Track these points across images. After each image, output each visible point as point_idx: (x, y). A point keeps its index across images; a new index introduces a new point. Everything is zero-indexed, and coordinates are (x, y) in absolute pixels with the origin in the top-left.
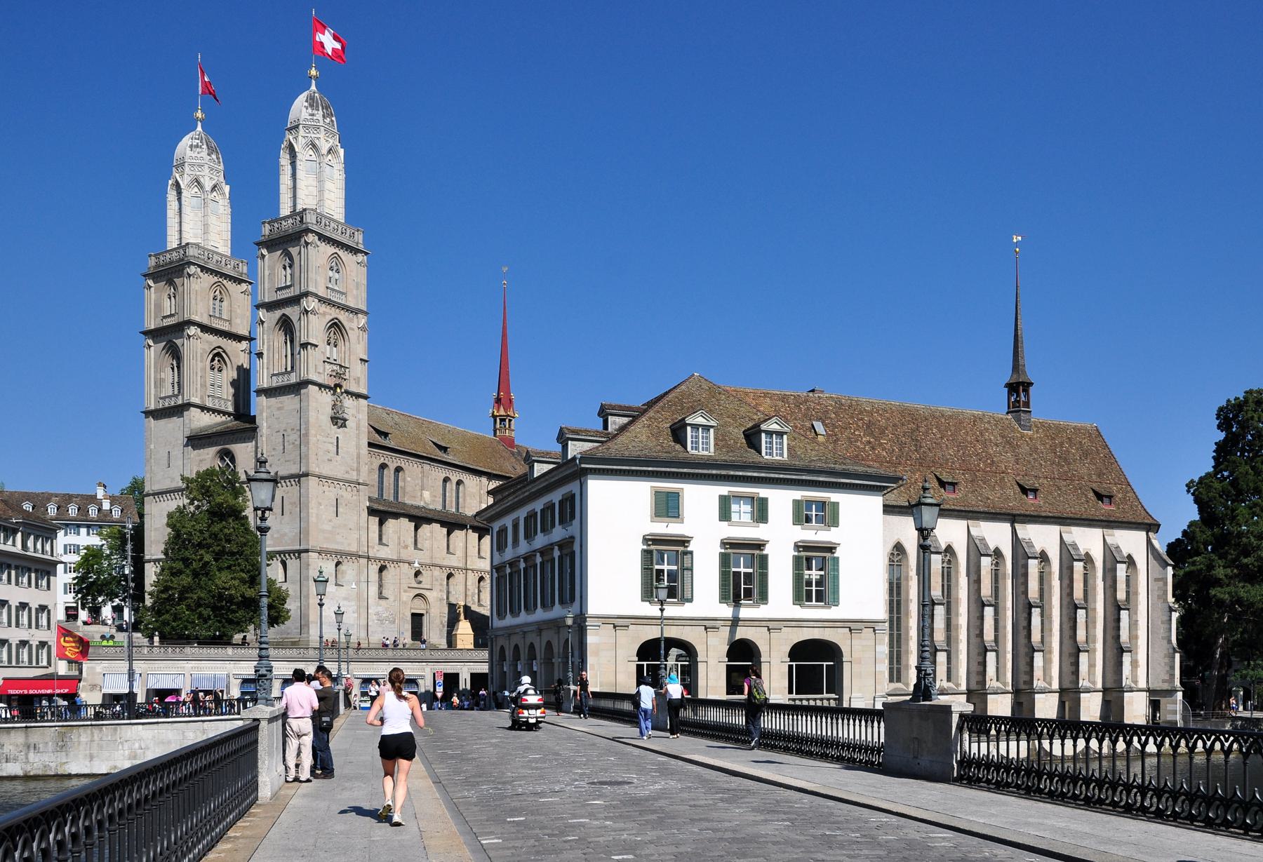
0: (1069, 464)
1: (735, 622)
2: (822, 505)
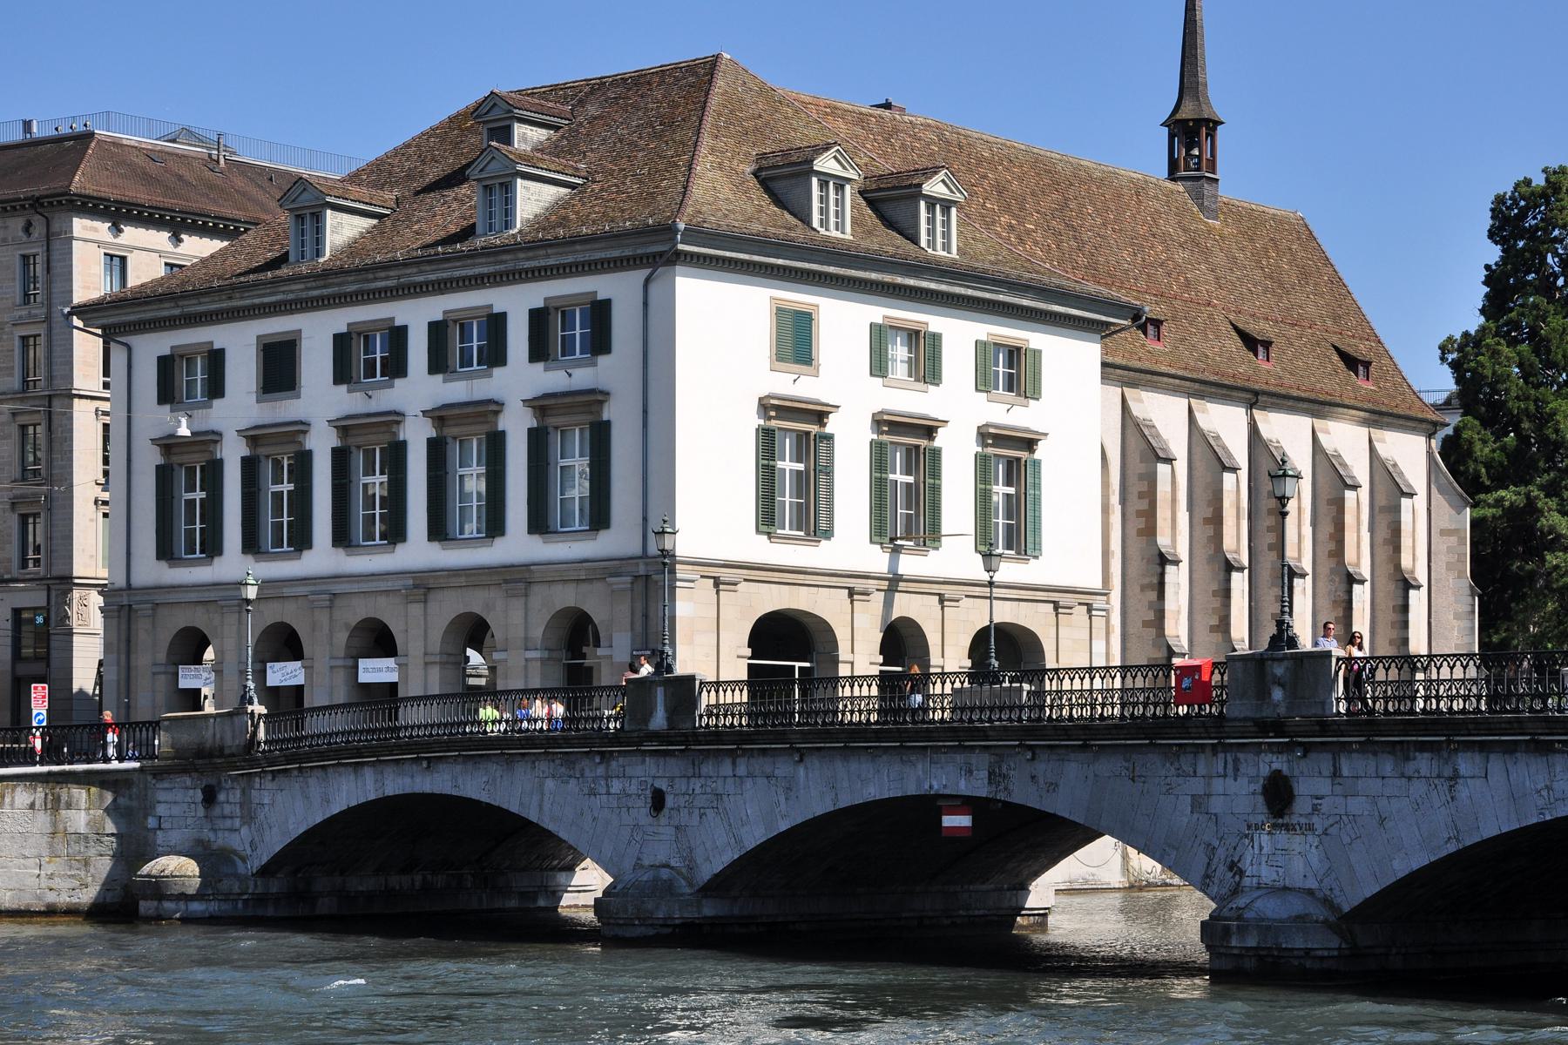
0: (1288, 293)
1: (894, 583)
2: (1014, 354)
